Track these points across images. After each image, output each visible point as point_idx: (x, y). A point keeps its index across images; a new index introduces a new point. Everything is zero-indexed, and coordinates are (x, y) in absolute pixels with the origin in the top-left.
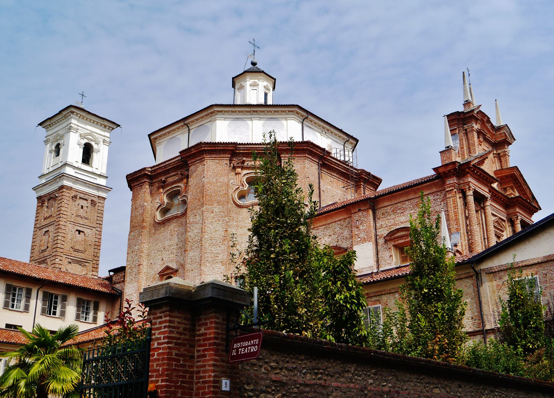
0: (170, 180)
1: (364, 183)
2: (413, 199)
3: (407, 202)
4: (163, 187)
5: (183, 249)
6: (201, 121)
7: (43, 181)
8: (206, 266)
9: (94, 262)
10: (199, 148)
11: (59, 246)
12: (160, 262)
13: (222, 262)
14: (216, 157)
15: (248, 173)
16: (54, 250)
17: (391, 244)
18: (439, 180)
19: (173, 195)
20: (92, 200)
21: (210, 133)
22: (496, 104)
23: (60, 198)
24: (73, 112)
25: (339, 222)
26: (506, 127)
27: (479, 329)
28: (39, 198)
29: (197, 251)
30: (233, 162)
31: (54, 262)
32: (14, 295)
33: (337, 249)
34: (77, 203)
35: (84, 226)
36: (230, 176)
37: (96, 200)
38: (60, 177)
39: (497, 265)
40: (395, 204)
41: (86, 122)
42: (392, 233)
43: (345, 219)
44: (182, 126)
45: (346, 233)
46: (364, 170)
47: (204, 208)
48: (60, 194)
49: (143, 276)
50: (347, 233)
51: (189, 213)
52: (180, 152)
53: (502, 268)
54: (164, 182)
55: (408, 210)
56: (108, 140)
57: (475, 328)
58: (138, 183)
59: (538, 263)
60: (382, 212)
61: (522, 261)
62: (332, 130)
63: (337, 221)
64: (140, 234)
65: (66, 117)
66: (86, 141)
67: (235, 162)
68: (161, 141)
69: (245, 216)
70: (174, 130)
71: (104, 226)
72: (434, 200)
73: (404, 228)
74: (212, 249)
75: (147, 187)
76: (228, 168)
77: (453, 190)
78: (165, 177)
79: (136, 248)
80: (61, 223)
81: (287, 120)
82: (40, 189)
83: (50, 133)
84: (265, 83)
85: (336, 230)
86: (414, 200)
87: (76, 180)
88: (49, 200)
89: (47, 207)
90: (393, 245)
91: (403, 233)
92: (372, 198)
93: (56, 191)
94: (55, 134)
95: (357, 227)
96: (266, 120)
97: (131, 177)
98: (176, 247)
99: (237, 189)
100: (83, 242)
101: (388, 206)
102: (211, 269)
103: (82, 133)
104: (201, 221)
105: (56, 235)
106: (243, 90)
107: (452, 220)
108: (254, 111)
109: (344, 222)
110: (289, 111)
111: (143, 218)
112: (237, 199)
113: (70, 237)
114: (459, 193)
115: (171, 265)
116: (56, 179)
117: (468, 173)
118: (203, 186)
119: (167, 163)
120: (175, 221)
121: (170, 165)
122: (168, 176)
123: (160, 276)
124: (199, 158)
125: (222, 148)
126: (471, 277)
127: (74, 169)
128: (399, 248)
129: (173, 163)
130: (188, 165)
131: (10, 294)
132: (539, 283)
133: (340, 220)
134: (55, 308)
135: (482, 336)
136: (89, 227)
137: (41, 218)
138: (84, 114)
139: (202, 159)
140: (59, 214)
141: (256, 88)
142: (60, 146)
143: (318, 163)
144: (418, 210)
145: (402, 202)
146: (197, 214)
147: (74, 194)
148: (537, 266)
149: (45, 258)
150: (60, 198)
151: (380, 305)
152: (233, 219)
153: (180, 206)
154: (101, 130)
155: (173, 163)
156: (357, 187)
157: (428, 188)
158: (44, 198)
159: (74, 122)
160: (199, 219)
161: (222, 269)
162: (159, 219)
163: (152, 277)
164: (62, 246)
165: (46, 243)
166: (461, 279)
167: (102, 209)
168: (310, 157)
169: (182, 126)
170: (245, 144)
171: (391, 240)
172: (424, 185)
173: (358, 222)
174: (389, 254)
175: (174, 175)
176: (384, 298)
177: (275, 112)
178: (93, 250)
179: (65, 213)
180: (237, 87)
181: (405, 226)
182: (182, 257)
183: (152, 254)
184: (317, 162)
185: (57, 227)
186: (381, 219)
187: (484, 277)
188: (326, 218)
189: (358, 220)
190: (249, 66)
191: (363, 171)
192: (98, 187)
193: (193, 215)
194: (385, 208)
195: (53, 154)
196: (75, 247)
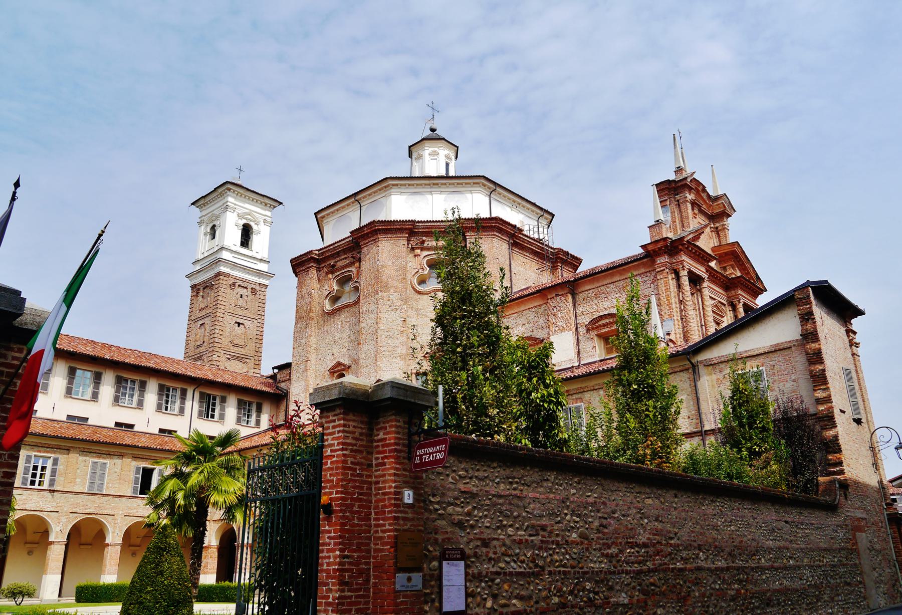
0: (340, 264)
1: (562, 263)
4: (332, 273)
5: (356, 342)
7: (198, 267)
8: (382, 361)
9: (256, 358)
11: (216, 340)
12: (330, 357)
13: (400, 356)
15: (428, 255)
16: (211, 345)
17: (593, 334)
19: (344, 281)
20: (252, 288)
21: (385, 209)
22: (712, 170)
23: (216, 286)
24: (229, 189)
25: (533, 309)
26: (725, 197)
27: (696, 430)
28: (193, 287)
30: (412, 242)
31: (211, 358)
32: (168, 396)
34: (236, 291)
35: (244, 318)
36: (408, 259)
37: (257, 288)
38: (217, 263)
39: (717, 356)
41: (244, 200)
42: (594, 321)
43: (540, 305)
44: (353, 203)
45: (542, 321)
46: (561, 249)
47: (380, 295)
48: (217, 282)
49: (311, 373)
50: (543, 322)
51: (362, 301)
52: (351, 233)
53: (723, 360)
54: (333, 266)
55: (612, 294)
56: (269, 219)
57: (692, 429)
58: (304, 268)
59: (765, 353)
60: (583, 297)
61: (746, 351)
62: (524, 203)
64: (307, 326)
65: (221, 195)
66: (244, 221)
67: (414, 242)
69: (426, 304)
70: (343, 207)
71: (266, 317)
72: (642, 282)
73: (609, 314)
74: (389, 341)
75: (315, 272)
76: (405, 249)
77: (664, 270)
78: (334, 261)
79: (303, 341)
80: (218, 314)
81: (472, 193)
82: (195, 276)
83: (204, 213)
84: (446, 152)
85: (530, 318)
86: (620, 282)
87: (234, 265)
88: (204, 289)
89: (203, 297)
90: (596, 335)
91: (607, 321)
92: (572, 281)
93: (212, 278)
94: (210, 215)
96: (449, 194)
97: (296, 261)
98: (348, 340)
99: (416, 273)
100: (243, 336)
102: (389, 364)
103: (240, 212)
104: (376, 310)
105: (213, 328)
106: (421, 160)
108: (434, 184)
110: (474, 183)
111: (311, 307)
112: (417, 285)
113: (229, 330)
114: (672, 273)
115: (342, 361)
116: (211, 265)
117: (681, 250)
118: (378, 271)
119: (336, 245)
120: (346, 310)
121: (340, 248)
122: (337, 259)
123: (330, 373)
124: (372, 239)
125: (398, 227)
126: (687, 370)
127: (231, 253)
128: (604, 338)
130: (360, 246)
131: (163, 395)
132: (765, 376)
133: (535, 307)
134: (213, 410)
135: (701, 437)
136: (249, 319)
137: (196, 309)
138: (241, 191)
140: (216, 305)
141: (436, 157)
142: (215, 228)
143: (509, 242)
144: (624, 294)
146: (372, 303)
147: (232, 281)
148: (763, 356)
149: (202, 354)
150: (216, 286)
151: (582, 404)
152: (412, 307)
153: (352, 293)
154: (261, 208)
156: (554, 268)
157: (635, 268)
158: (199, 287)
159: (231, 200)
161: (400, 365)
162: (328, 309)
164: (220, 341)
165: (202, 338)
166: (676, 372)
167: (264, 298)
168: (499, 235)
169: (353, 203)
170: (424, 222)
171: (593, 329)
172: (631, 265)
174: (592, 345)
175: (345, 258)
176: (587, 396)
177: (458, 184)
178: (254, 344)
179: (222, 303)
180: (414, 157)
181: (610, 313)
182: (355, 352)
184: (507, 241)
185: (214, 319)
186: (582, 305)
187: (702, 370)
188: (518, 305)
190: (428, 133)
191: (560, 250)
192: (259, 273)
194: (587, 293)
195: (208, 237)
196: (234, 342)
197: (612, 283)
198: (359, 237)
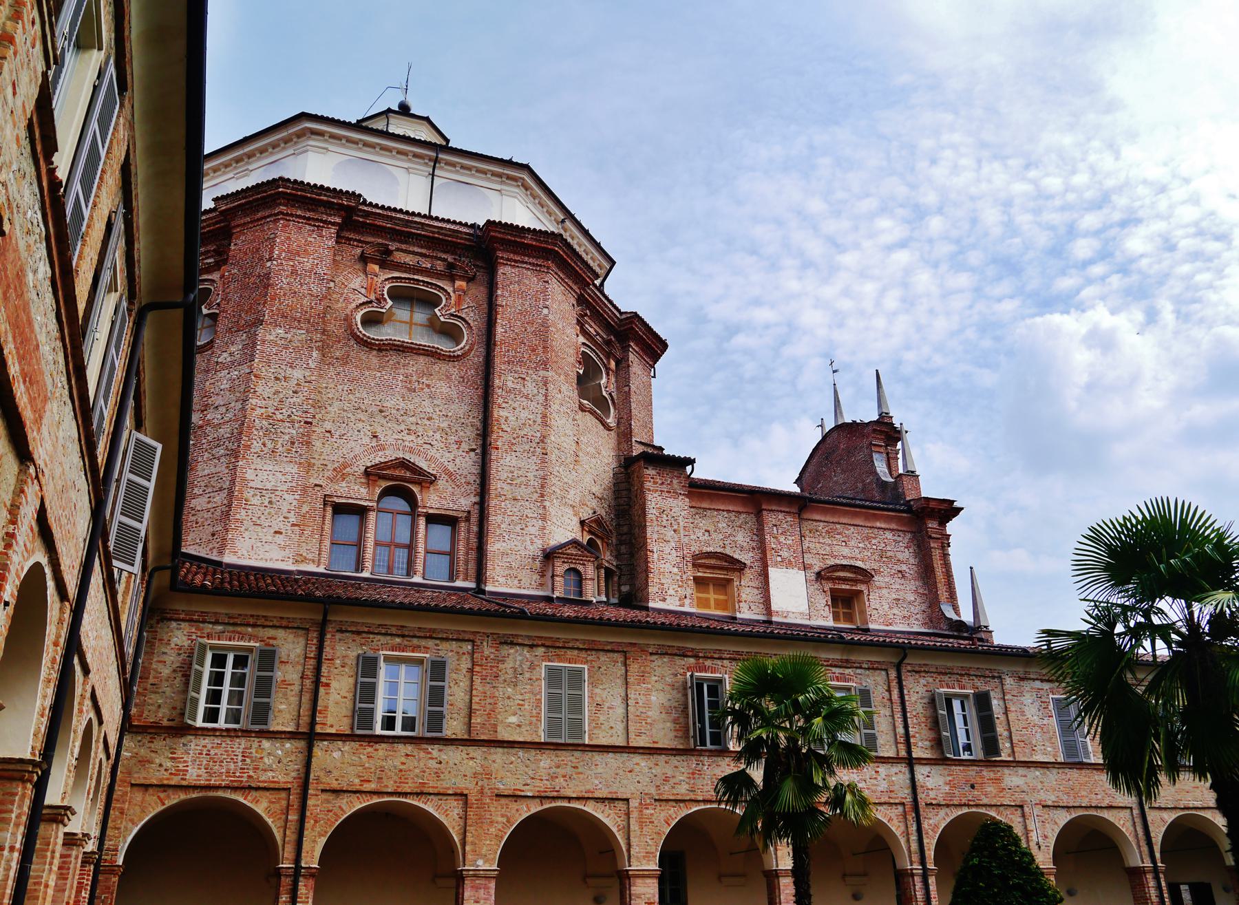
2: (861, 526)
3: (852, 528)
4: (384, 265)
6: (473, 176)
10: (546, 242)
14: (563, 280)
17: (828, 586)
18: (909, 515)
29: (530, 461)
33: (726, 561)
40: (833, 523)
45: (742, 538)
60: (809, 527)
63: (723, 511)
68: (331, 148)
70: (384, 148)
73: (851, 566)
95: (776, 538)
97: (296, 190)
101: (821, 521)
104: (541, 398)
107: (940, 582)
109: (736, 517)
115: (413, 458)
129: (436, 230)
133: (728, 511)
139: (540, 266)
145: (845, 524)
155: (436, 230)
160: (535, 391)
163: (330, 467)
171: (829, 579)
173: (775, 528)
183: (329, 408)
189: (776, 526)
193: (516, 375)
194: (815, 523)
197: (853, 525)
198: (503, 242)
